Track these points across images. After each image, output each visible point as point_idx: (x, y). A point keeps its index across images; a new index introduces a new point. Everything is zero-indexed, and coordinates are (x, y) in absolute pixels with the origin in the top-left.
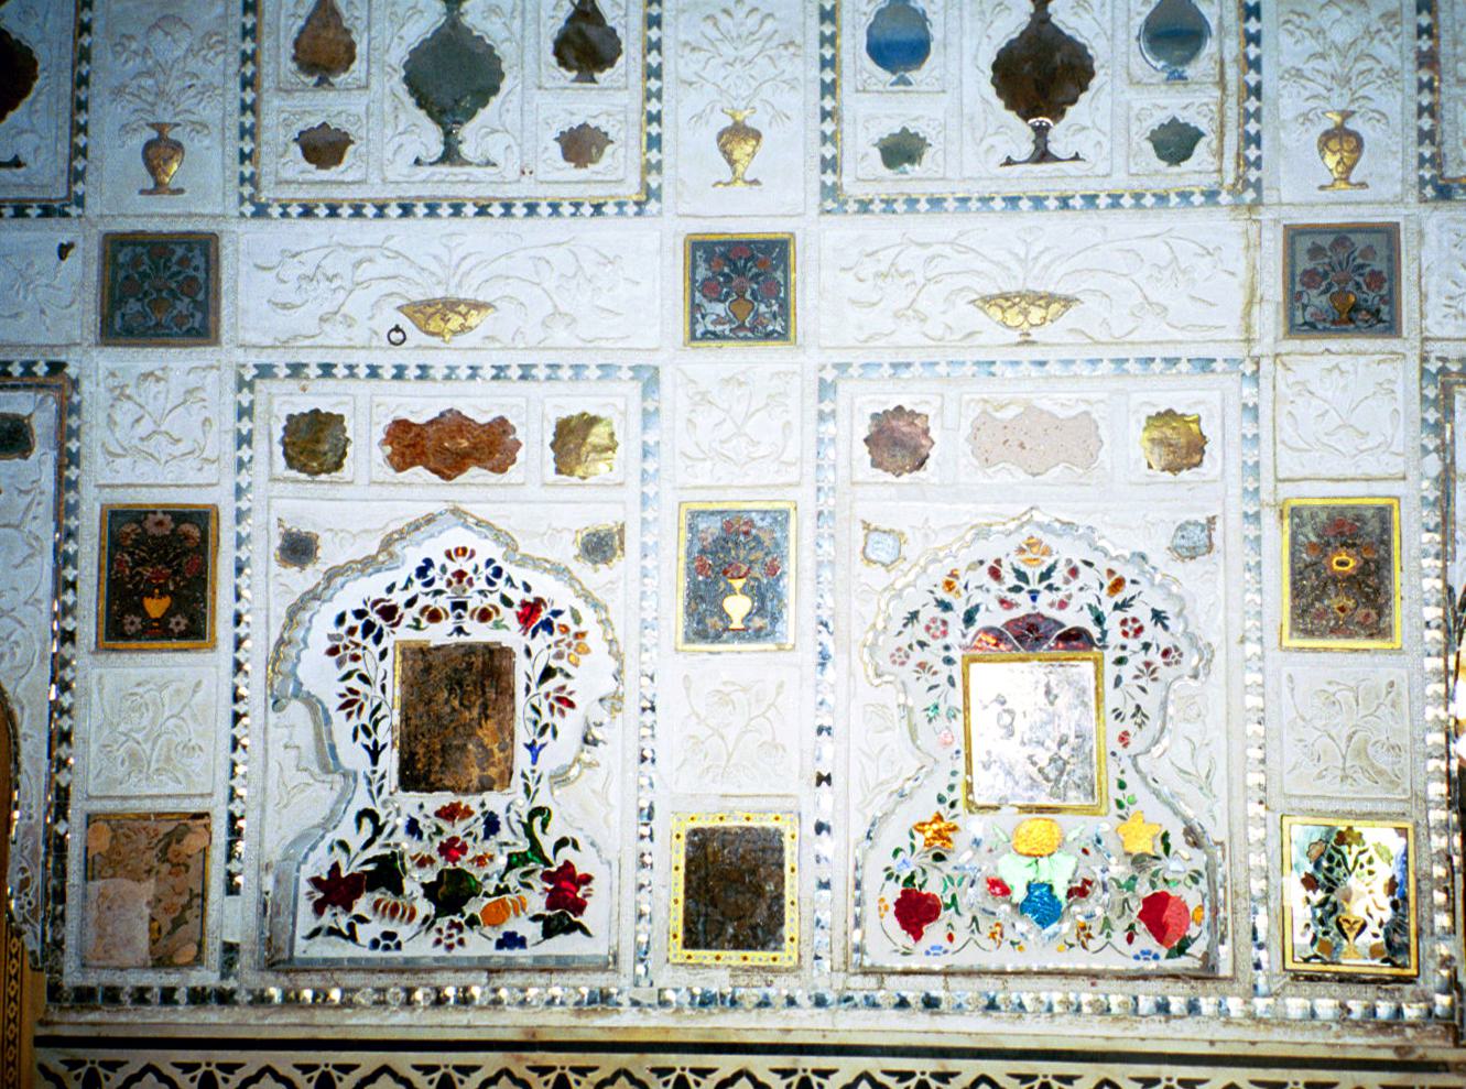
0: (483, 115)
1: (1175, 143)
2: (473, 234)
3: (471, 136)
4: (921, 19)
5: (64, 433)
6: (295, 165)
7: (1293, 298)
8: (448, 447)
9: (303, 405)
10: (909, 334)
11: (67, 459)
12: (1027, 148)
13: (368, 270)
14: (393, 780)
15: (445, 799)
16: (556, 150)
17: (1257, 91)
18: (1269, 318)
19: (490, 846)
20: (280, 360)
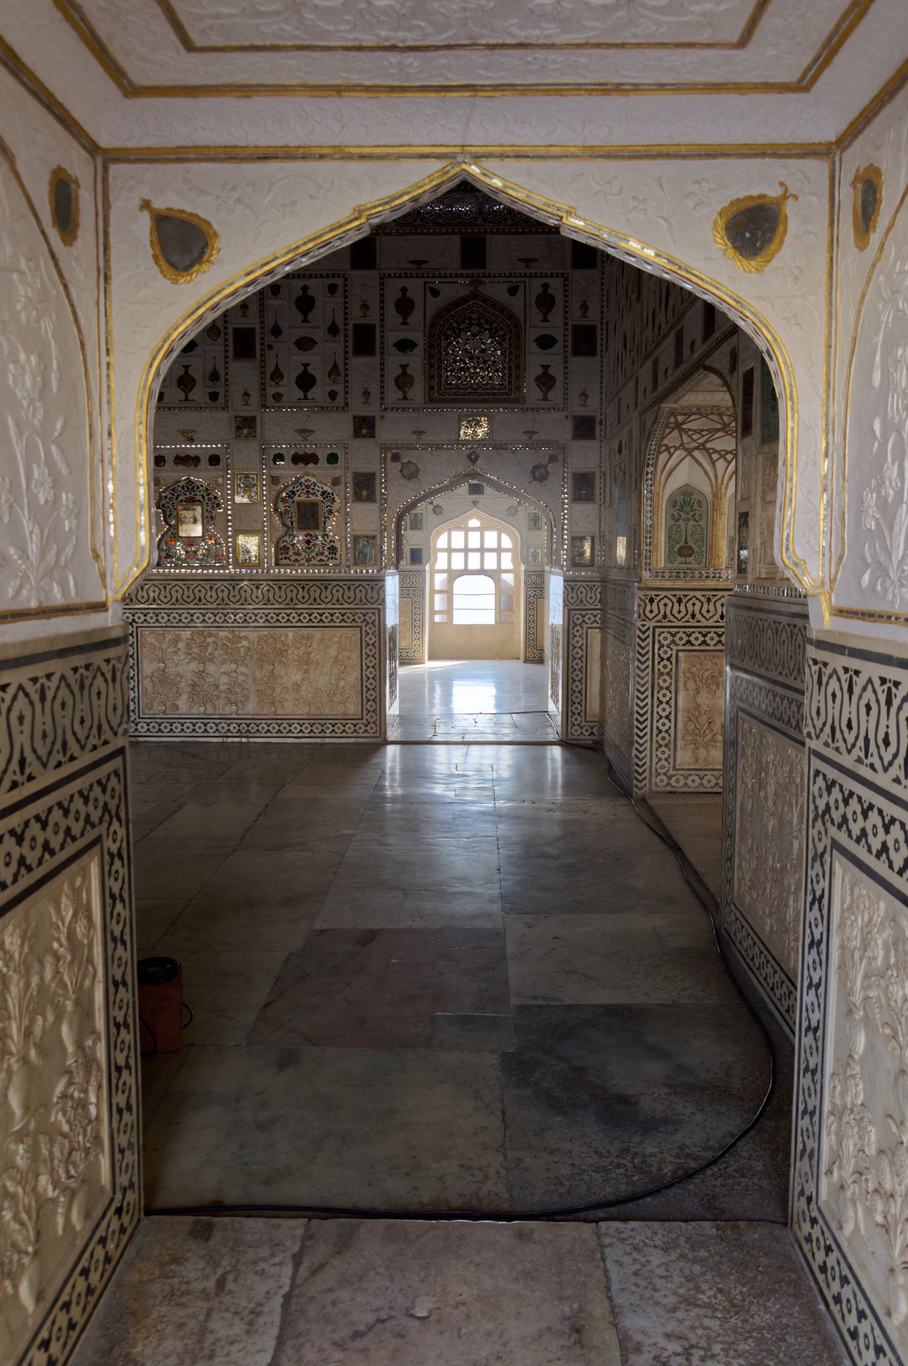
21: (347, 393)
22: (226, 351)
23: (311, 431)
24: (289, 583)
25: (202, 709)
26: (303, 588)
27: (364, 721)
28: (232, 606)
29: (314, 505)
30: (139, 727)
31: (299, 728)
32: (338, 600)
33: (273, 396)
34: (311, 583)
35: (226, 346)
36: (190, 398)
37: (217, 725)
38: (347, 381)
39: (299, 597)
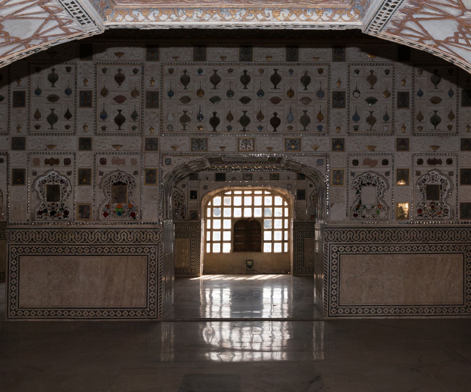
0: (56, 124)
1: (134, 128)
2: (55, 138)
3: (54, 126)
4: (106, 113)
5: (8, 160)
6: (34, 129)
7: (146, 146)
8: (53, 162)
9: (35, 157)
10: (104, 149)
11: (8, 163)
12: (118, 128)
13: (42, 141)
14: (46, 200)
15: (52, 202)
16: (64, 128)
17: (143, 123)
18: (144, 148)
19: (57, 208)
20: (32, 152)
21: (458, 126)
22: (393, 104)
23: (439, 147)
24: (425, 229)
25: (374, 300)
26: (433, 232)
27: (465, 306)
28: (393, 242)
29: (436, 186)
30: (339, 311)
31: (428, 310)
32: (451, 239)
33: (418, 128)
34: (437, 229)
35: (393, 101)
36: (373, 129)
37: (382, 309)
38: (458, 120)
39: (430, 237)
